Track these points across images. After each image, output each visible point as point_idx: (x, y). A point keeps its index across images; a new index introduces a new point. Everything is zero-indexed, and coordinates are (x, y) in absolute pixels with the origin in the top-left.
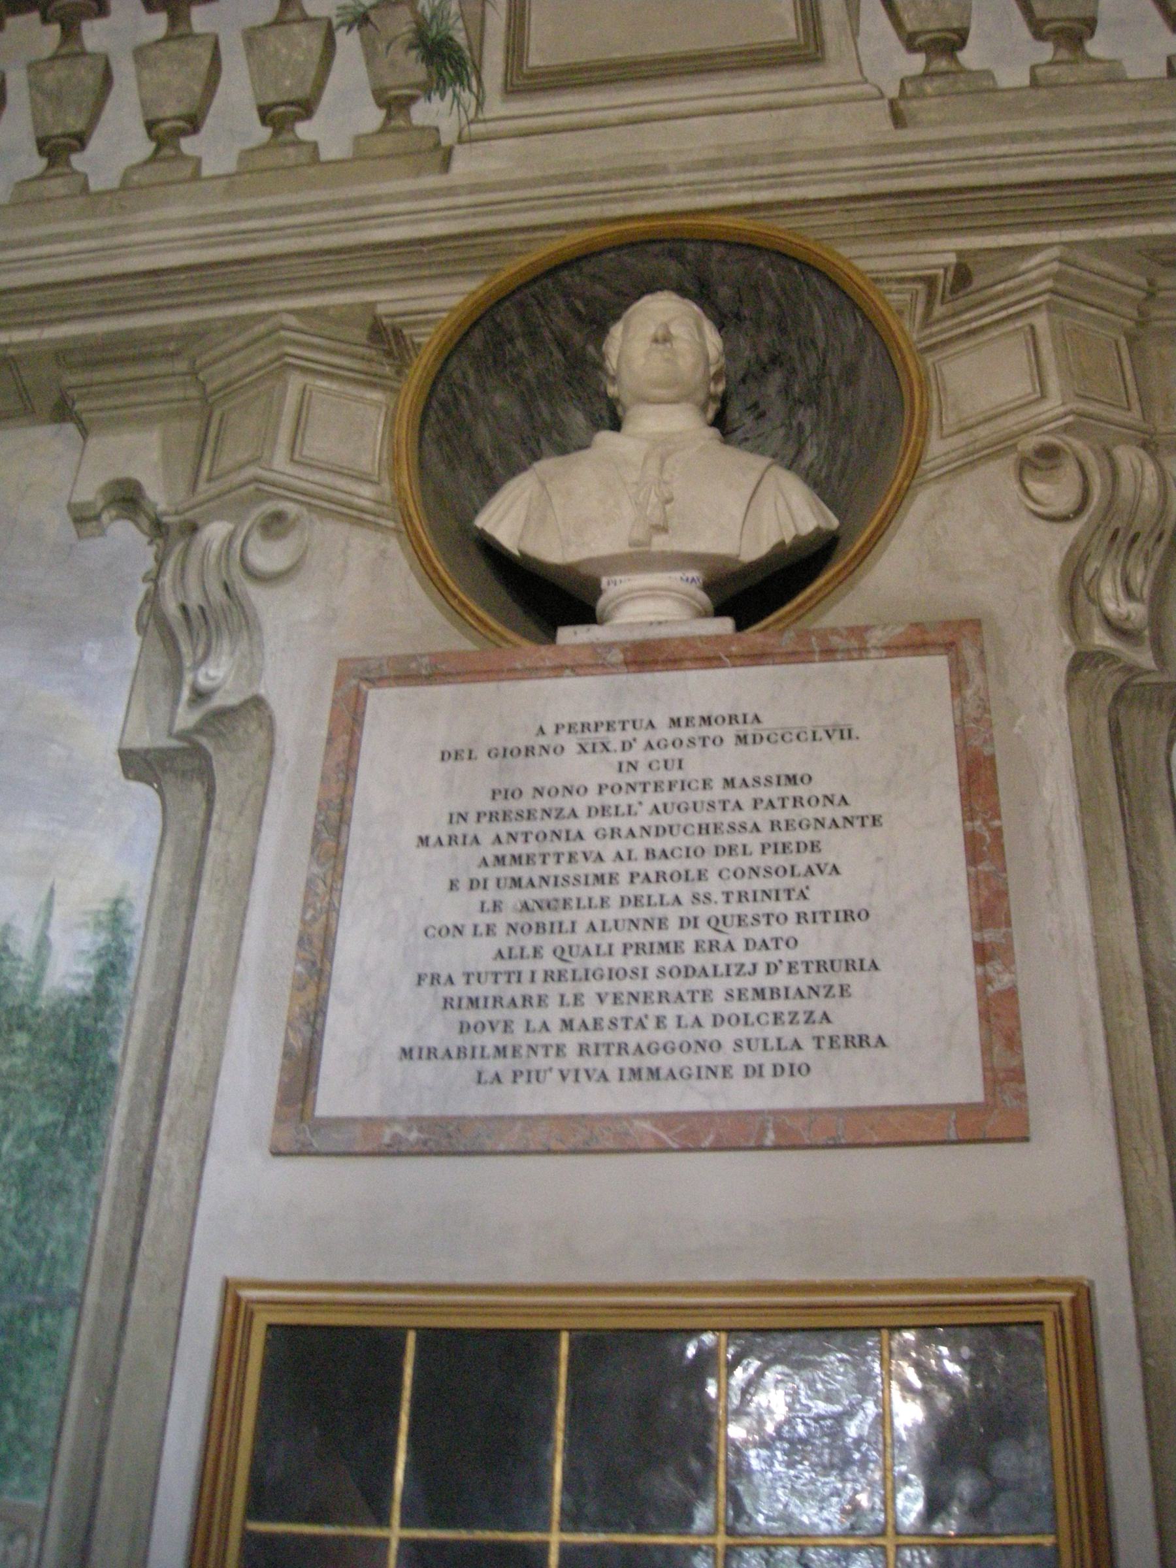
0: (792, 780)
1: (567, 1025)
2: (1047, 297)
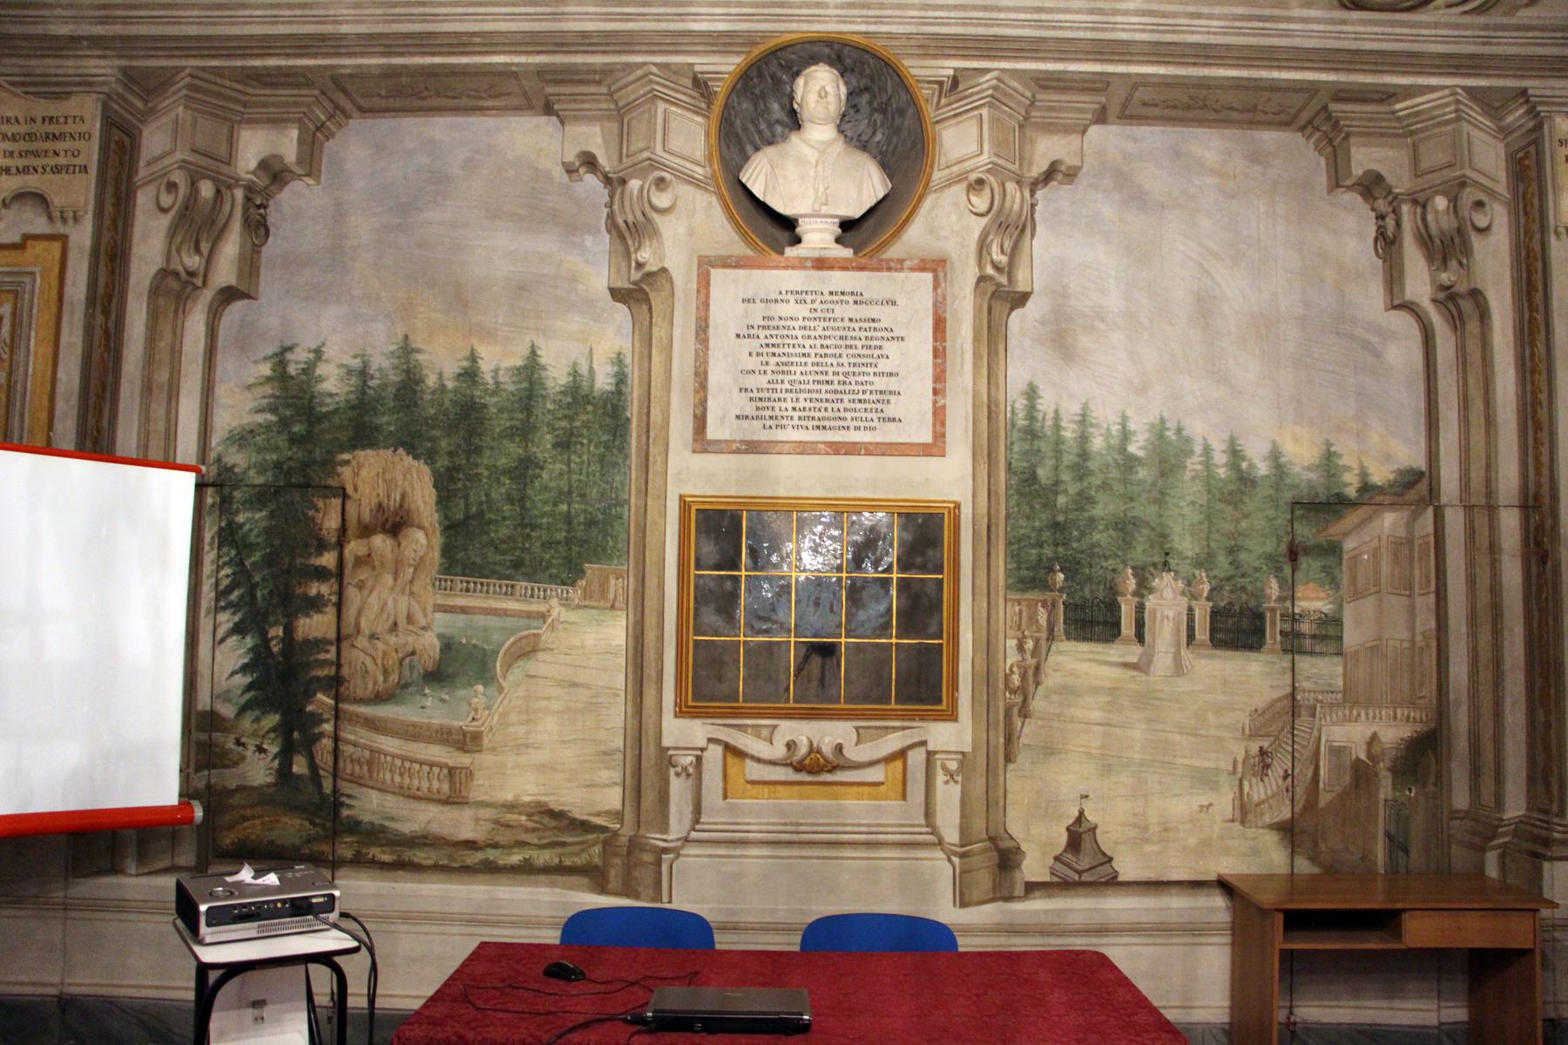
0: (873, 320)
1: (794, 409)
2: (989, 99)
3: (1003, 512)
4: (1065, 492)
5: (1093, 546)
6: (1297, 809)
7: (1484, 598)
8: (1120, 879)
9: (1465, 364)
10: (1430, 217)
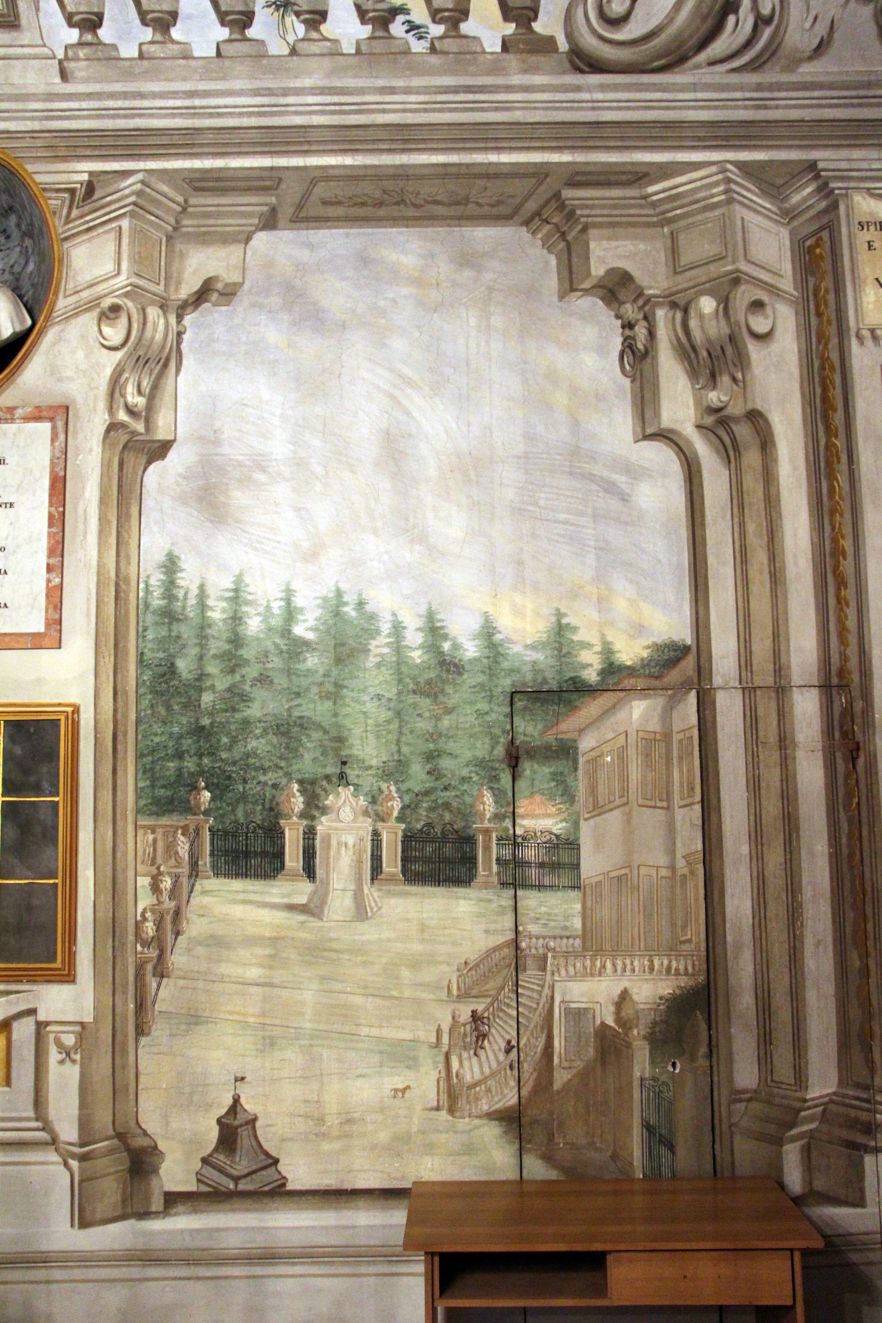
3: (133, 716)
4: (213, 687)
5: (248, 755)
6: (525, 1092)
7: (772, 807)
8: (290, 1187)
9: (742, 506)
10: (693, 323)
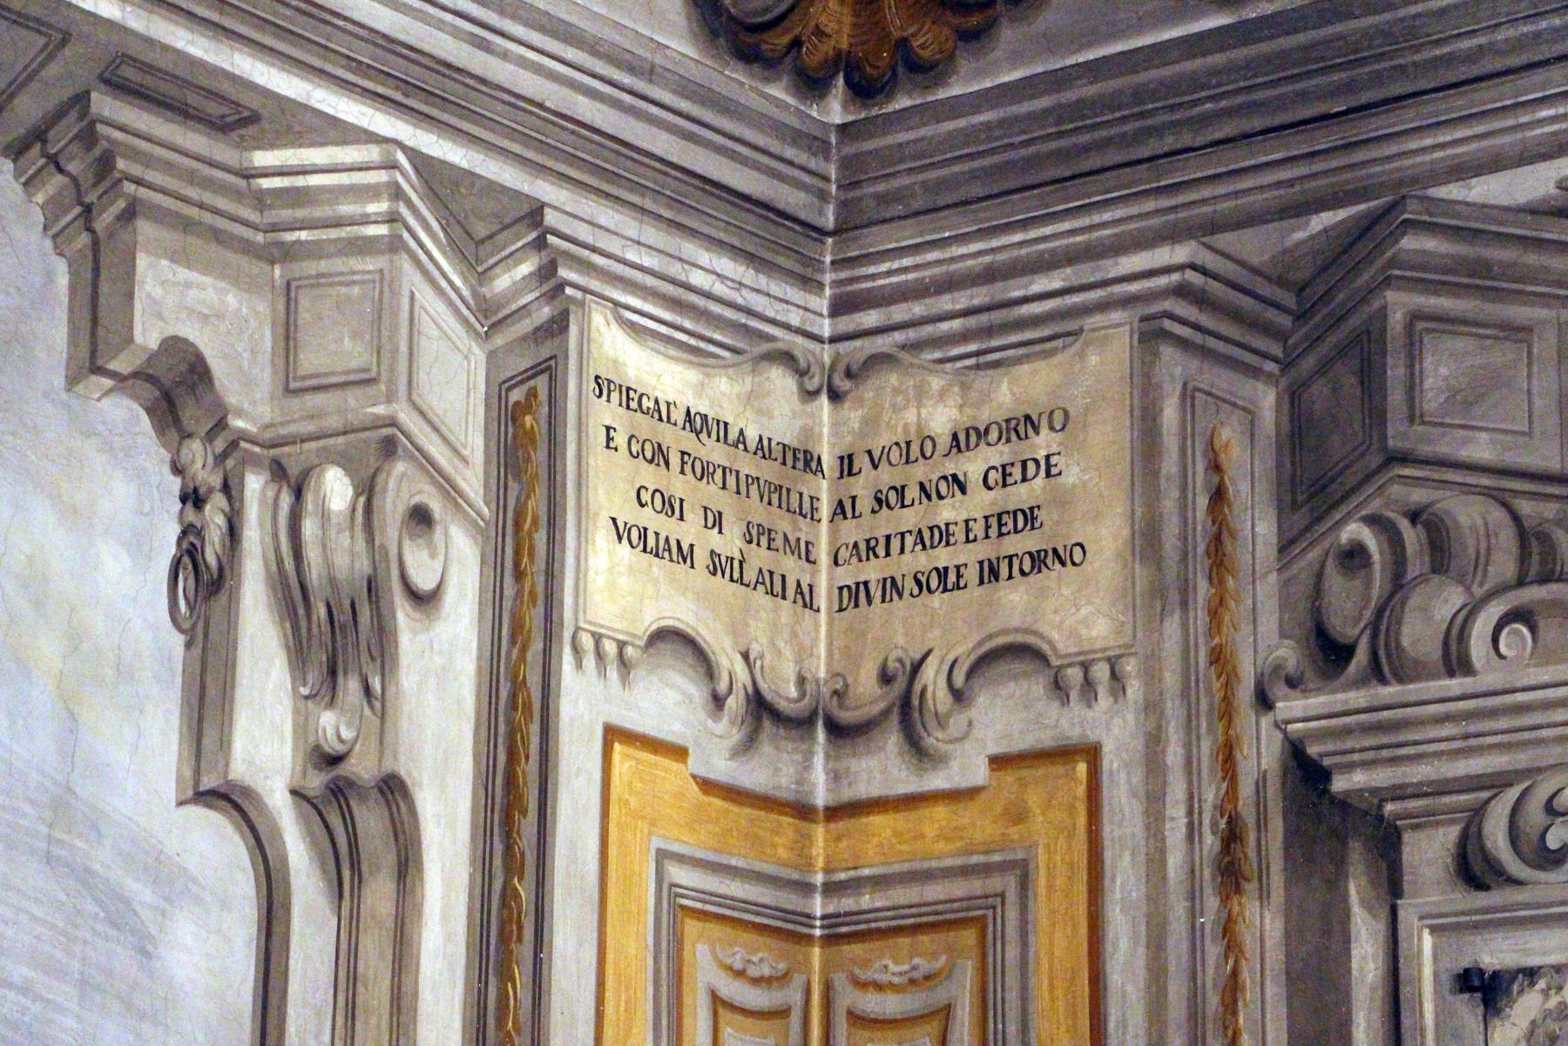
10: (309, 528)
